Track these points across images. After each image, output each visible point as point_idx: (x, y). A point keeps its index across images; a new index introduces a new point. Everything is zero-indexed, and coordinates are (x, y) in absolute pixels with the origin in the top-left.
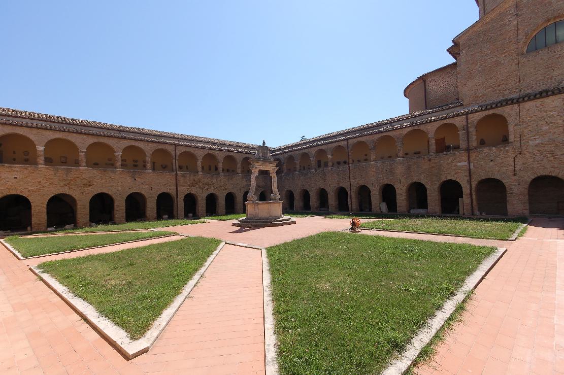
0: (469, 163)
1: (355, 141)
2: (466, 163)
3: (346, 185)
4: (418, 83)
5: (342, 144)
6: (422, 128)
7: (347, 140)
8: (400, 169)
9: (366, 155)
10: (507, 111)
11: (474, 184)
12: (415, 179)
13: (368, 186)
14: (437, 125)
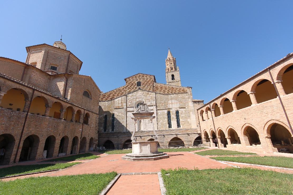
0: (82, 130)
1: (40, 94)
2: (81, 130)
3: (15, 132)
4: (21, 64)
5: (27, 90)
6: (74, 107)
7: (34, 90)
8: (61, 126)
9: (10, 104)
10: (90, 113)
11: (82, 138)
12: (66, 135)
13: (39, 136)
14: (78, 109)
